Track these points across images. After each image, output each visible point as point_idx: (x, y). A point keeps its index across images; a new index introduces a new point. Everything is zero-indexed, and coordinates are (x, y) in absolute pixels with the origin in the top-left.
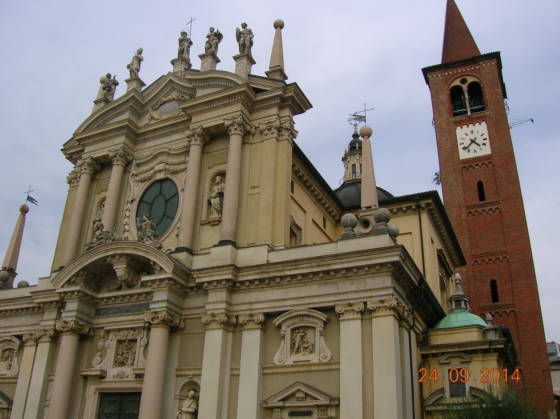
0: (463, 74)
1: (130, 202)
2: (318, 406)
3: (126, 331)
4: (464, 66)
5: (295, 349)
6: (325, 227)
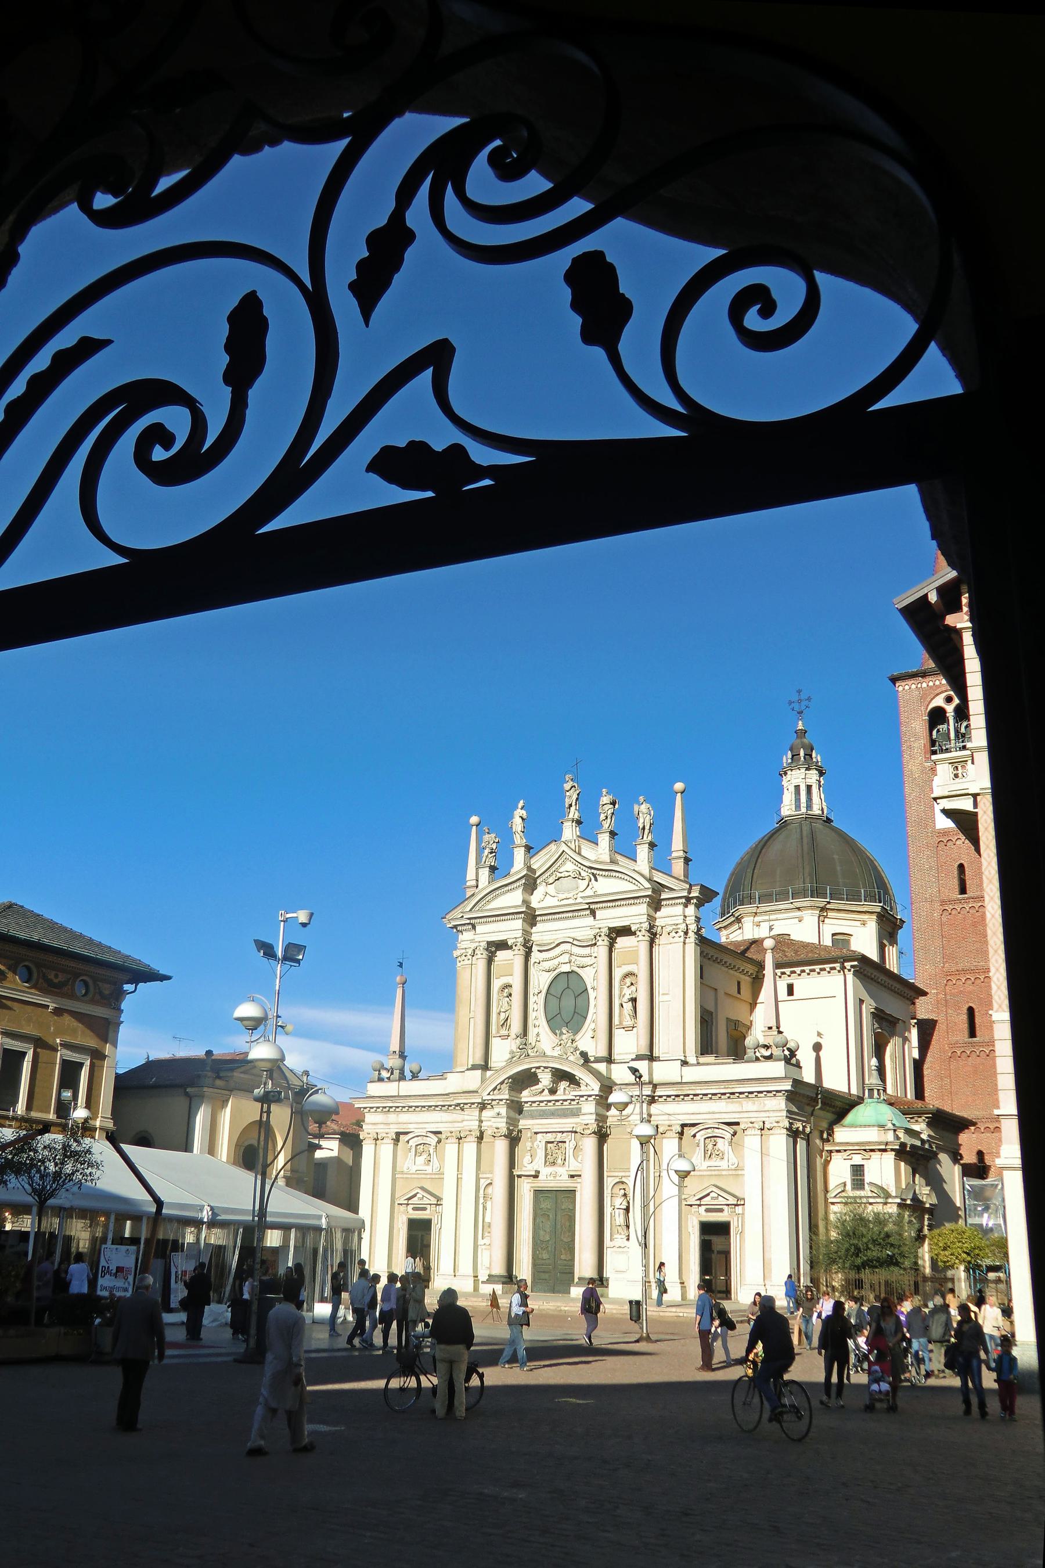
2: (728, 1205)
3: (554, 1134)
5: (708, 1155)
6: (739, 992)
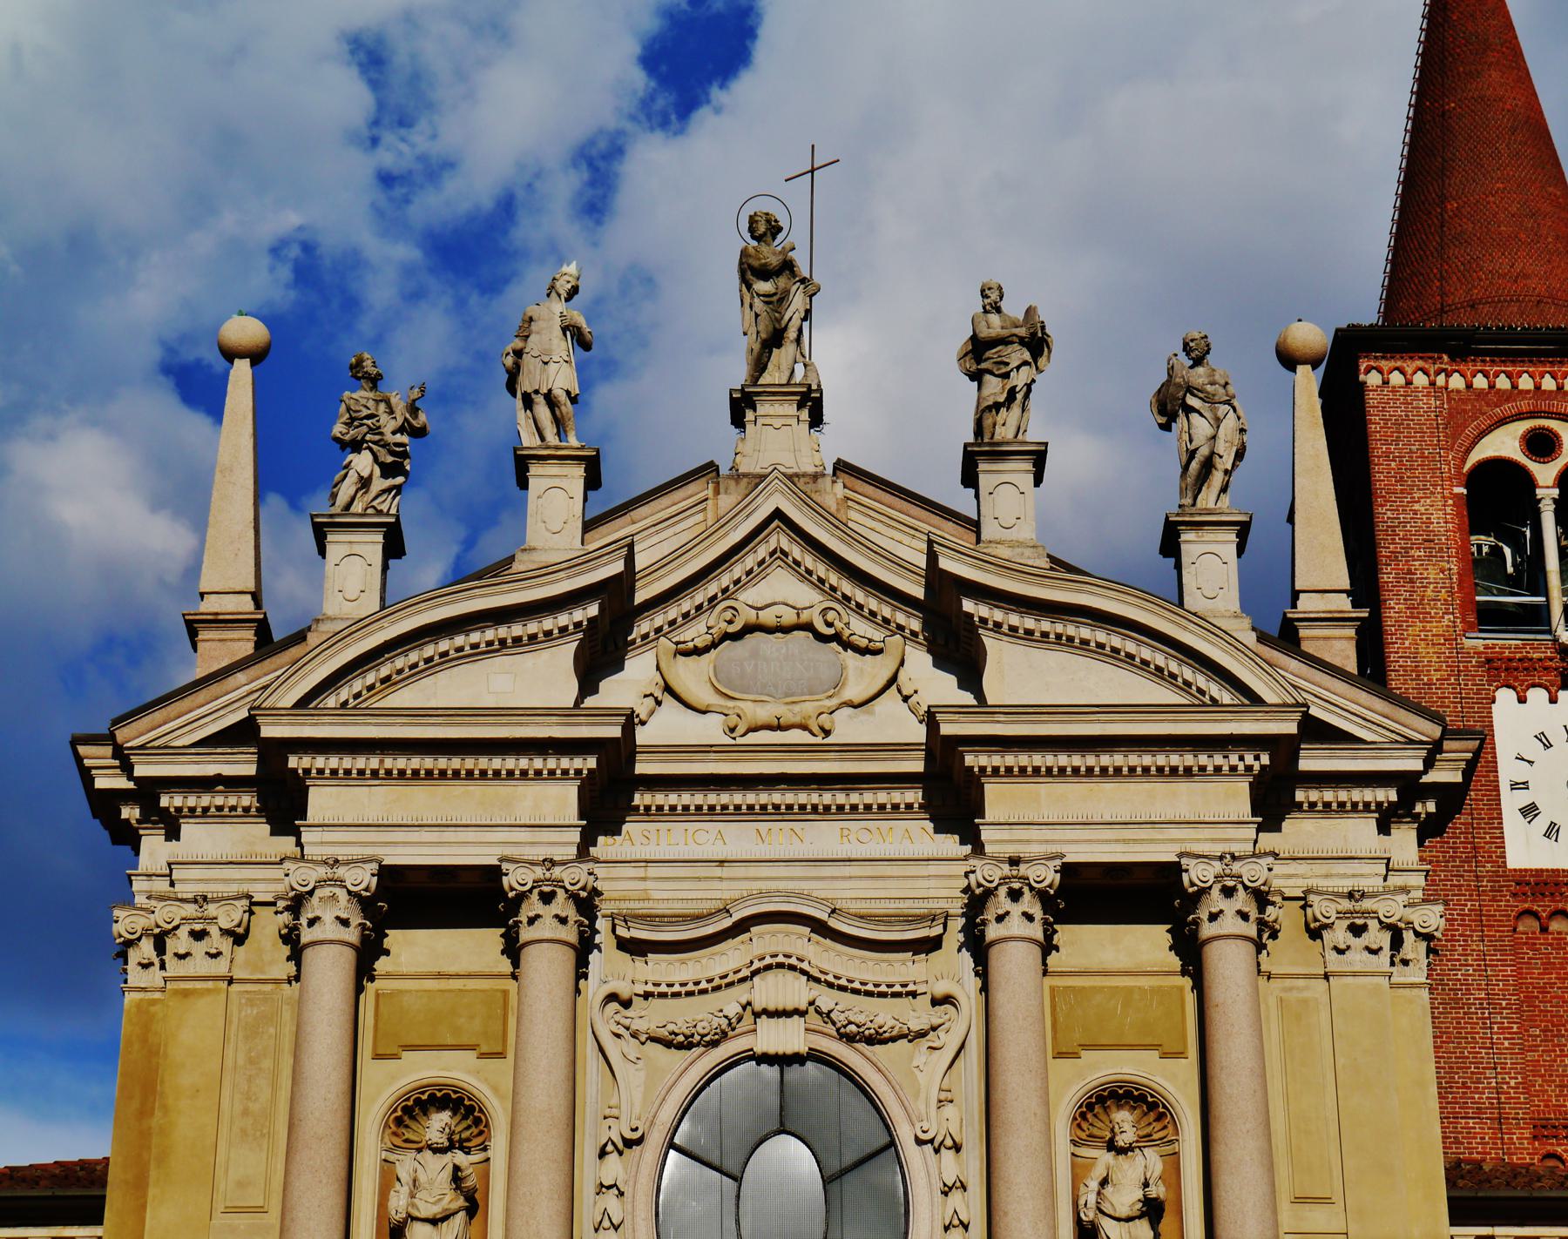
0: (1543, 406)
1: (620, 1145)
4: (1552, 364)
